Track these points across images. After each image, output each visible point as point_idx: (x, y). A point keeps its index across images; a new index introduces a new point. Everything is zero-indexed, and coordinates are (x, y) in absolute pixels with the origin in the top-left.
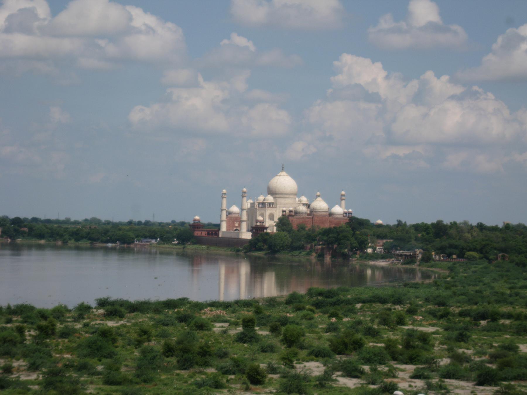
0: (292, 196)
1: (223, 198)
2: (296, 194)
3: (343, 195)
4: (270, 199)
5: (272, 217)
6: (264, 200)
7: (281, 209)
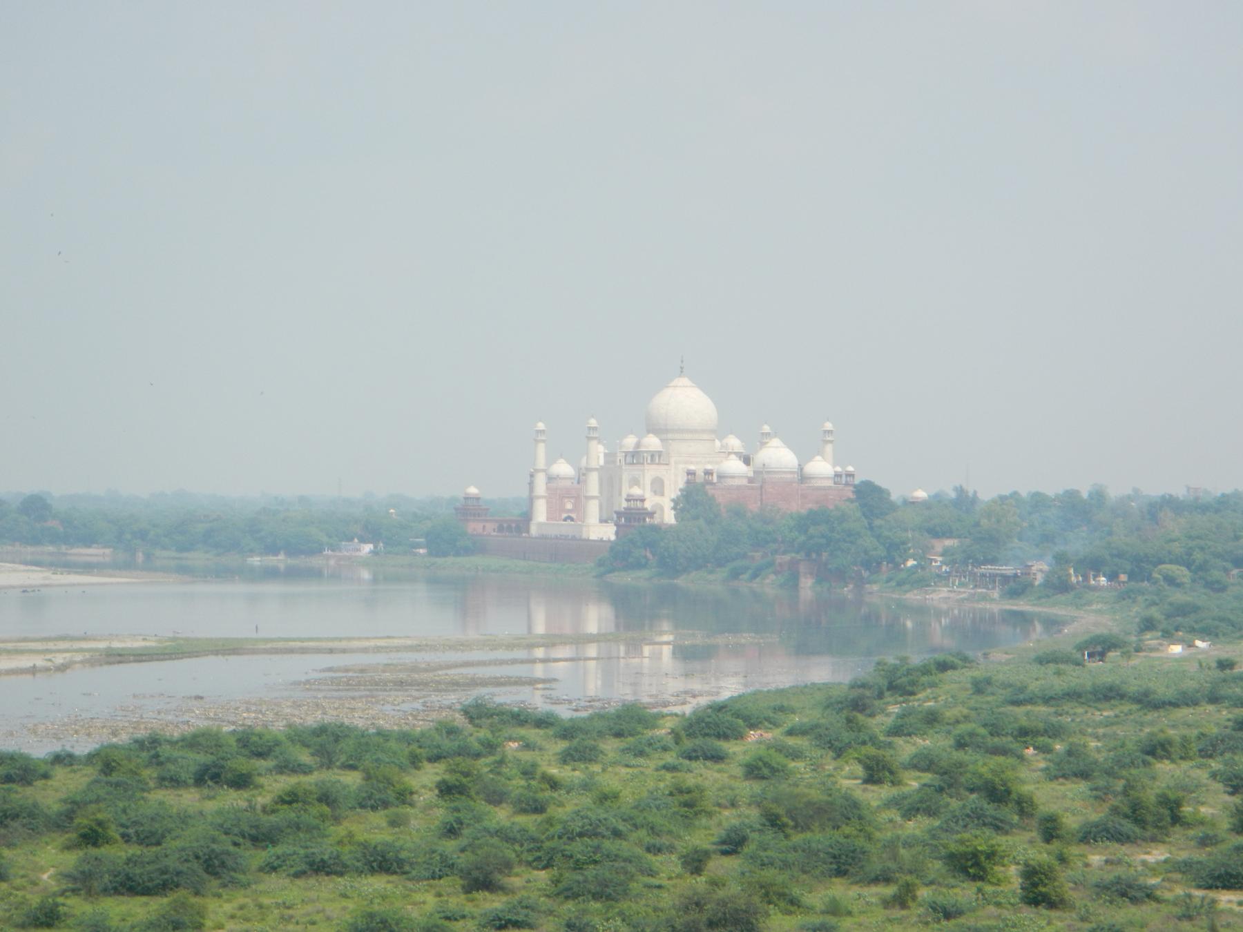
0: (705, 436)
1: (537, 441)
2: (713, 431)
3: (830, 432)
4: (652, 442)
5: (658, 486)
6: (638, 445)
7: (681, 466)
